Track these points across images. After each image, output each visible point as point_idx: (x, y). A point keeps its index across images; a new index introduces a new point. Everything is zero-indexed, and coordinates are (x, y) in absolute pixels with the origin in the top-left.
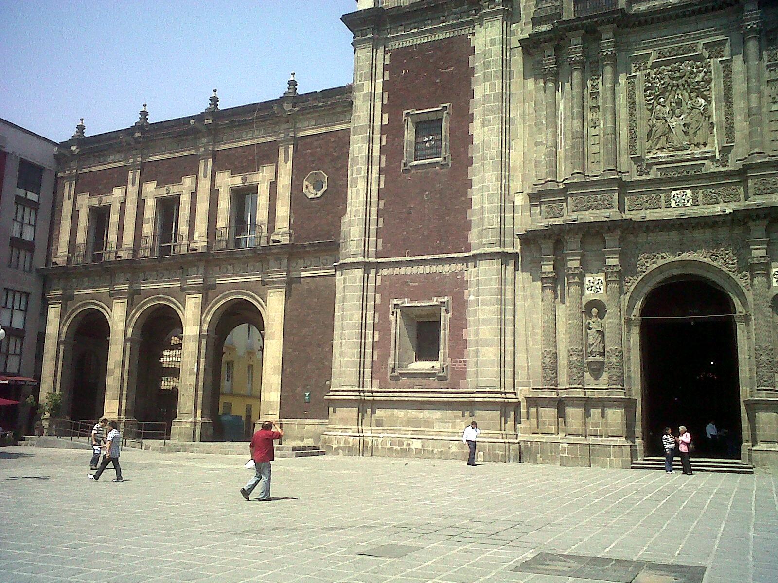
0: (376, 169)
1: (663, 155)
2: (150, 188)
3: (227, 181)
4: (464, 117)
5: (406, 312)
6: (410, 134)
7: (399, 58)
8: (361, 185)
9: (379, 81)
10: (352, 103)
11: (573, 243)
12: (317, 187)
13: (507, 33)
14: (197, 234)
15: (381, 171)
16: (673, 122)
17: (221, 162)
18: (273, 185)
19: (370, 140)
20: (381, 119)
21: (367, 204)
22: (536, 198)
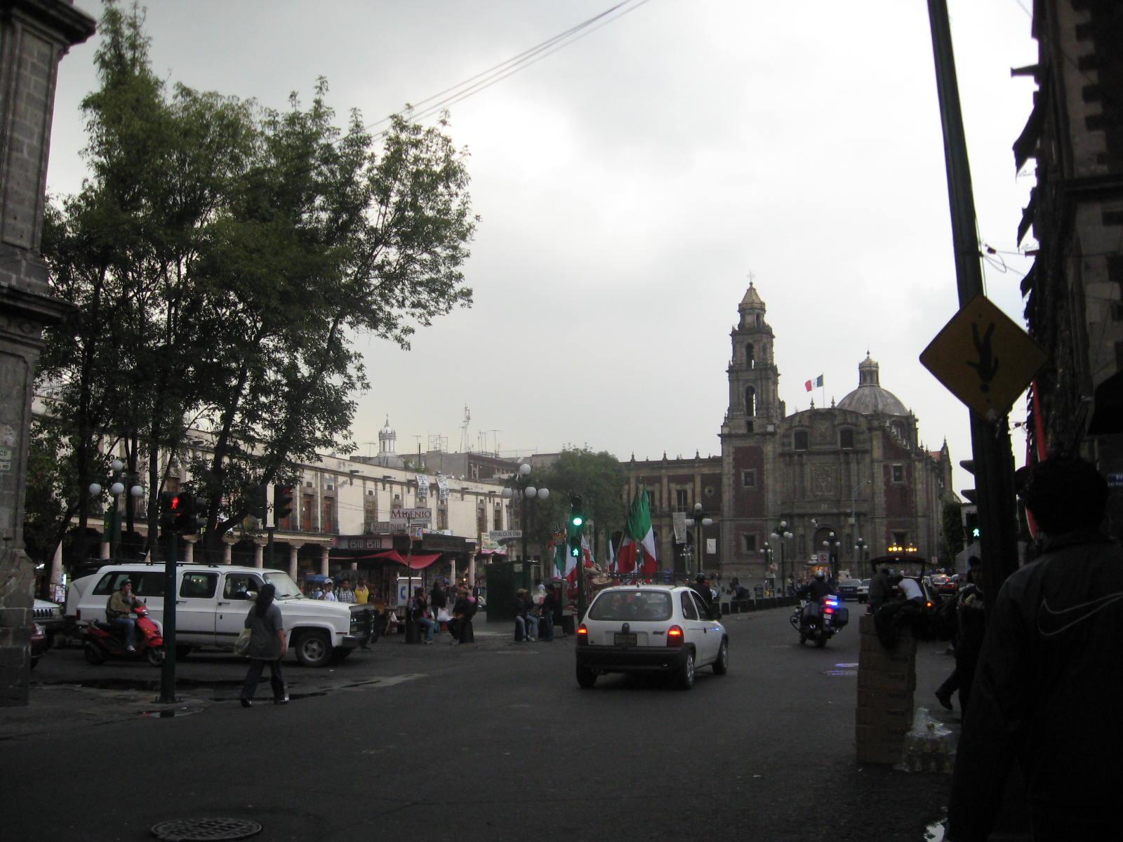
0: (731, 488)
1: (819, 494)
2: (641, 486)
3: (674, 487)
4: (761, 472)
5: (744, 535)
6: (743, 478)
7: (738, 451)
8: (727, 494)
9: (731, 458)
10: (722, 465)
11: (796, 519)
12: (710, 491)
13: (775, 448)
14: (664, 506)
15: (734, 489)
16: (822, 484)
17: (672, 479)
18: (693, 491)
19: (729, 479)
20: (733, 471)
21: (729, 500)
22: (783, 503)
